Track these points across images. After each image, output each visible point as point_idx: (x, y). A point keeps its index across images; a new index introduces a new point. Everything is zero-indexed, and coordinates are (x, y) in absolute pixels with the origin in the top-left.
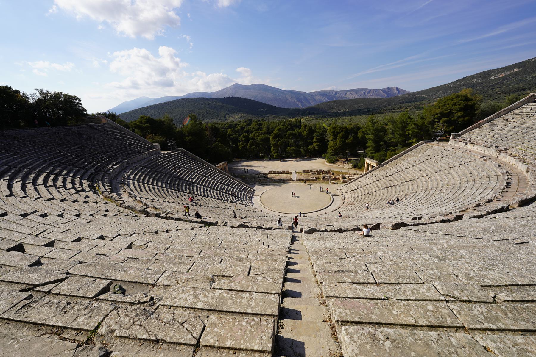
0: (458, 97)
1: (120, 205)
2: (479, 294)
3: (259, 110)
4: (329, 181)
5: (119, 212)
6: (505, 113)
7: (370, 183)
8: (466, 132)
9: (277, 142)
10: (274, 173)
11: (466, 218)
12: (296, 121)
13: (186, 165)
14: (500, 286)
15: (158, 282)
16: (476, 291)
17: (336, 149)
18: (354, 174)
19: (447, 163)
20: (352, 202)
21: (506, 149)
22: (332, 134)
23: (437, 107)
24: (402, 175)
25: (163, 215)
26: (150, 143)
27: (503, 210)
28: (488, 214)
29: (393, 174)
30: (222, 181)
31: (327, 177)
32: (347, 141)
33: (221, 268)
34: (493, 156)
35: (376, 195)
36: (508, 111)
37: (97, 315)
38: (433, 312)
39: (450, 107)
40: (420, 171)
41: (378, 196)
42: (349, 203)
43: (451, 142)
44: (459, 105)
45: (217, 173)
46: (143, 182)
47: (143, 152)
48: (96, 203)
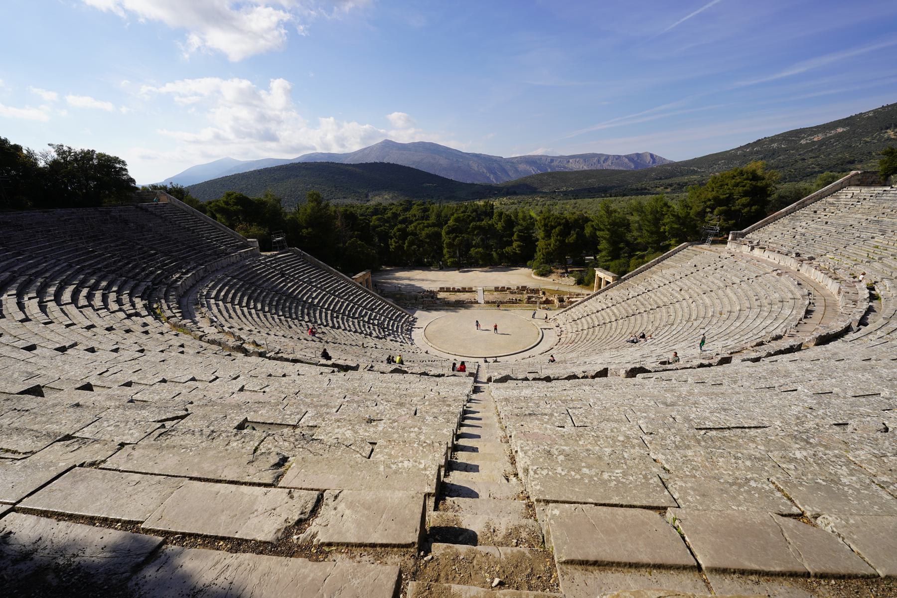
0: (741, 173)
1: (201, 338)
2: (687, 432)
3: (424, 185)
4: (538, 305)
5: (202, 349)
6: (813, 201)
7: (603, 310)
8: (753, 230)
9: (454, 240)
10: (448, 290)
11: (736, 360)
12: (486, 204)
13: (303, 275)
14: (722, 428)
15: (300, 423)
16: (685, 429)
17: (548, 254)
18: (578, 295)
19: (723, 279)
20: (573, 339)
21: (811, 259)
23: (710, 190)
24: (653, 296)
25: (272, 354)
26: (243, 238)
27: (791, 350)
28: (769, 355)
29: (638, 295)
30: (362, 303)
31: (533, 299)
32: (567, 241)
33: (378, 411)
34: (792, 268)
35: (611, 328)
36: (817, 198)
37: (251, 441)
38: (623, 441)
39: (729, 189)
40: (681, 290)
41: (614, 329)
42: (567, 340)
44: (744, 186)
45: (354, 289)
46: (232, 302)
47: (230, 253)
48: (162, 333)
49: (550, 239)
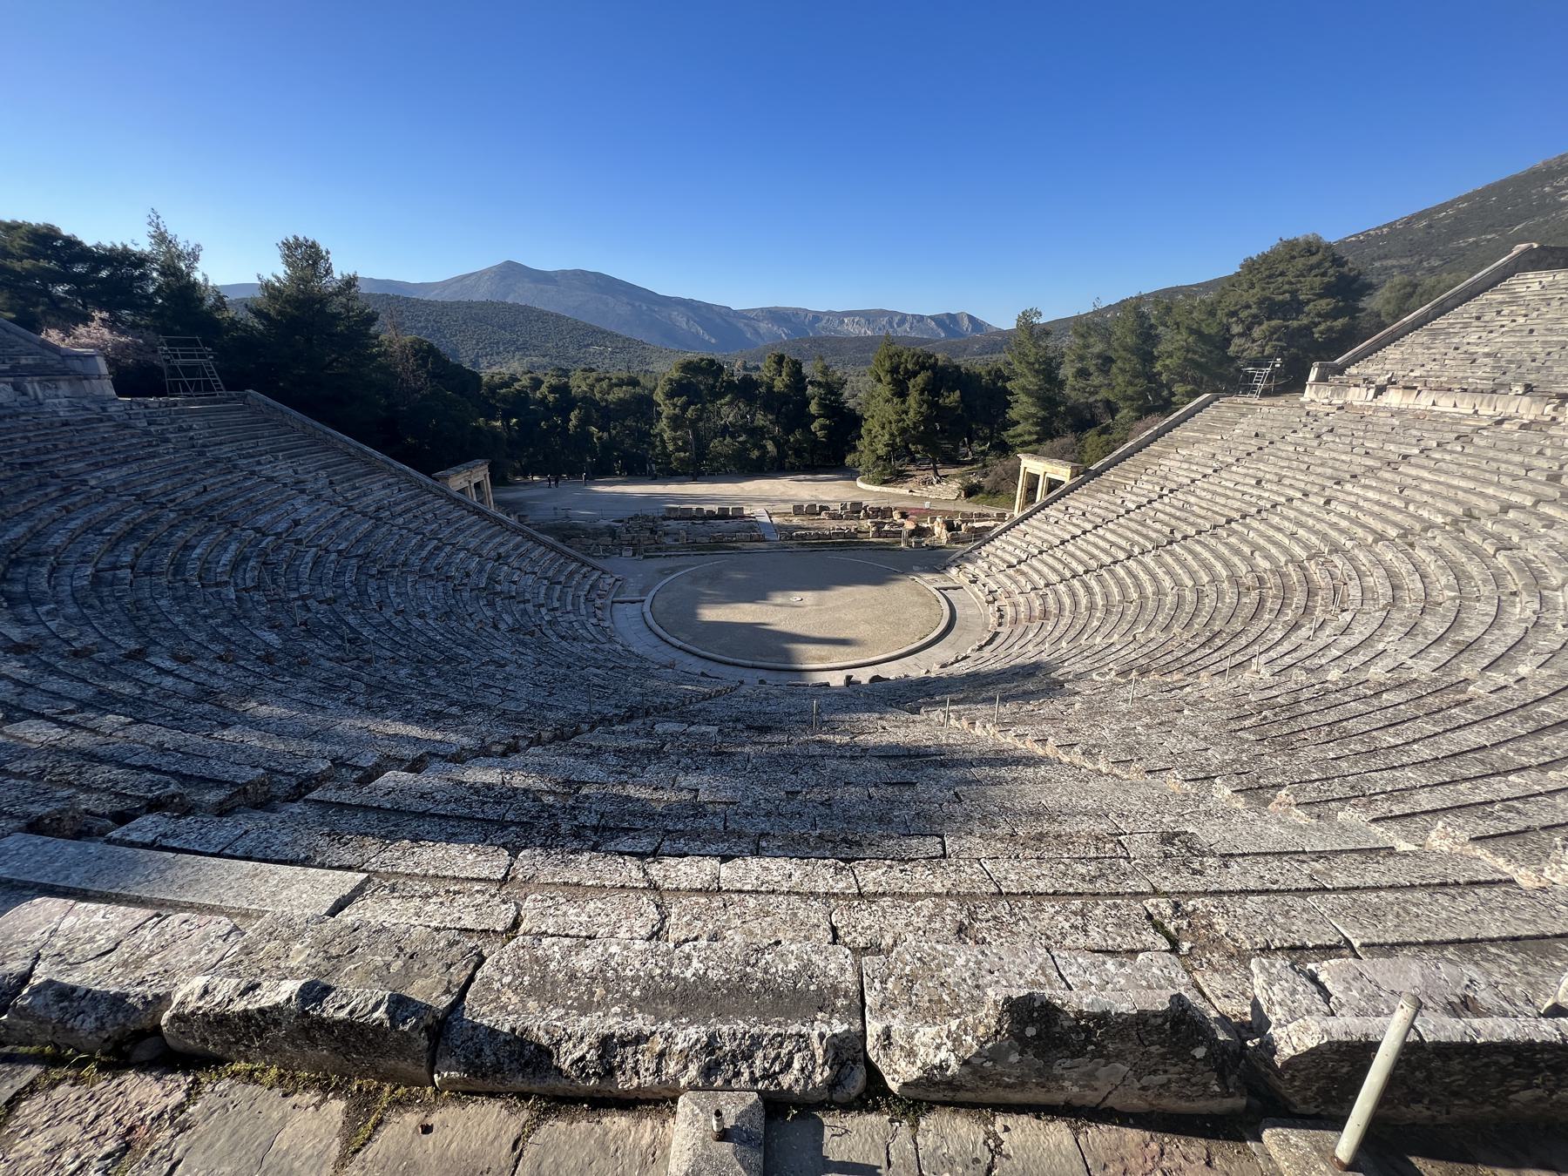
6: (1458, 301)
9: (684, 408)
17: (903, 431)
18: (981, 517)
22: (888, 378)
24: (1192, 499)
31: (886, 528)
39: (1290, 283)
40: (1259, 482)
43: (1314, 395)
49: (903, 402)
